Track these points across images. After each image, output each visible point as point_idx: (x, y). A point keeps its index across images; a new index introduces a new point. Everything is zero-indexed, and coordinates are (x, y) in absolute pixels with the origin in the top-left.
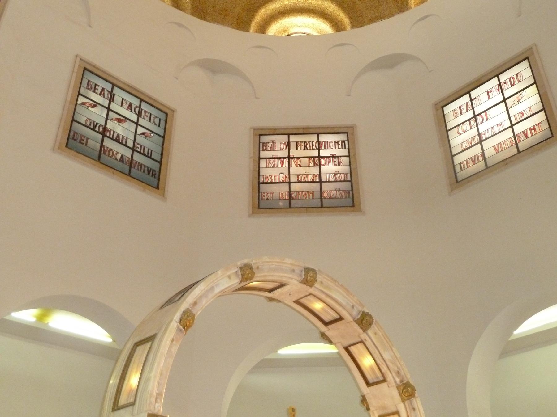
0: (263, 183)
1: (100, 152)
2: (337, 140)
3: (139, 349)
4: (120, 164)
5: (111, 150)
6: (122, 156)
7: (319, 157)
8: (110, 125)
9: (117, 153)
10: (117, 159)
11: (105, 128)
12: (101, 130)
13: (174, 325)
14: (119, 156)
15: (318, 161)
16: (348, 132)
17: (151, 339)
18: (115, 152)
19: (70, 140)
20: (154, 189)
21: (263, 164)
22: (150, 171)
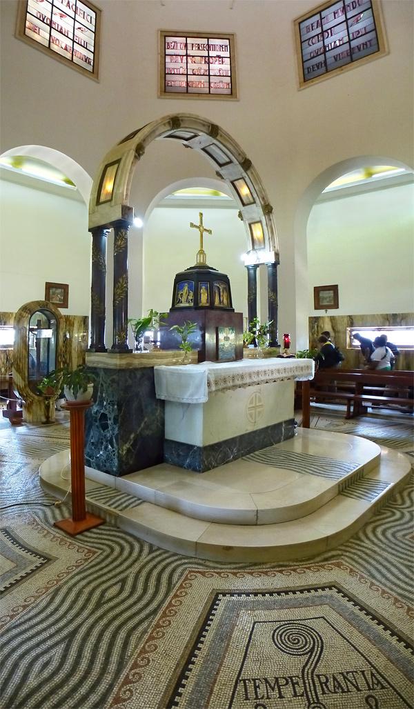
0: (168, 74)
2: (221, 44)
3: (109, 169)
7: (209, 56)
8: (56, 19)
11: (51, 21)
12: (48, 22)
13: (133, 153)
15: (208, 60)
16: (229, 37)
17: (118, 161)
21: (168, 59)
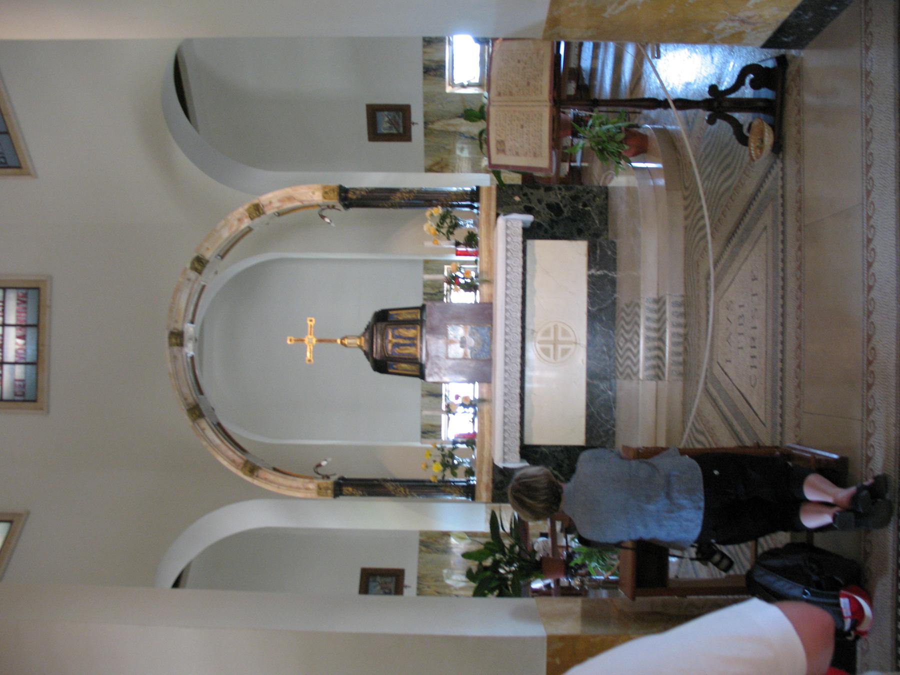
1: (26, 364)
4: (29, 337)
5: (16, 351)
6: (19, 337)
9: (17, 344)
10: (25, 344)
14: (21, 342)
18: (18, 347)
19: (27, 398)
20: (42, 292)
22: (22, 301)
